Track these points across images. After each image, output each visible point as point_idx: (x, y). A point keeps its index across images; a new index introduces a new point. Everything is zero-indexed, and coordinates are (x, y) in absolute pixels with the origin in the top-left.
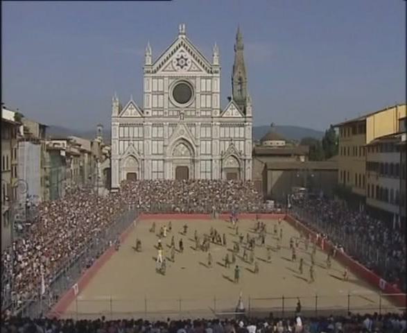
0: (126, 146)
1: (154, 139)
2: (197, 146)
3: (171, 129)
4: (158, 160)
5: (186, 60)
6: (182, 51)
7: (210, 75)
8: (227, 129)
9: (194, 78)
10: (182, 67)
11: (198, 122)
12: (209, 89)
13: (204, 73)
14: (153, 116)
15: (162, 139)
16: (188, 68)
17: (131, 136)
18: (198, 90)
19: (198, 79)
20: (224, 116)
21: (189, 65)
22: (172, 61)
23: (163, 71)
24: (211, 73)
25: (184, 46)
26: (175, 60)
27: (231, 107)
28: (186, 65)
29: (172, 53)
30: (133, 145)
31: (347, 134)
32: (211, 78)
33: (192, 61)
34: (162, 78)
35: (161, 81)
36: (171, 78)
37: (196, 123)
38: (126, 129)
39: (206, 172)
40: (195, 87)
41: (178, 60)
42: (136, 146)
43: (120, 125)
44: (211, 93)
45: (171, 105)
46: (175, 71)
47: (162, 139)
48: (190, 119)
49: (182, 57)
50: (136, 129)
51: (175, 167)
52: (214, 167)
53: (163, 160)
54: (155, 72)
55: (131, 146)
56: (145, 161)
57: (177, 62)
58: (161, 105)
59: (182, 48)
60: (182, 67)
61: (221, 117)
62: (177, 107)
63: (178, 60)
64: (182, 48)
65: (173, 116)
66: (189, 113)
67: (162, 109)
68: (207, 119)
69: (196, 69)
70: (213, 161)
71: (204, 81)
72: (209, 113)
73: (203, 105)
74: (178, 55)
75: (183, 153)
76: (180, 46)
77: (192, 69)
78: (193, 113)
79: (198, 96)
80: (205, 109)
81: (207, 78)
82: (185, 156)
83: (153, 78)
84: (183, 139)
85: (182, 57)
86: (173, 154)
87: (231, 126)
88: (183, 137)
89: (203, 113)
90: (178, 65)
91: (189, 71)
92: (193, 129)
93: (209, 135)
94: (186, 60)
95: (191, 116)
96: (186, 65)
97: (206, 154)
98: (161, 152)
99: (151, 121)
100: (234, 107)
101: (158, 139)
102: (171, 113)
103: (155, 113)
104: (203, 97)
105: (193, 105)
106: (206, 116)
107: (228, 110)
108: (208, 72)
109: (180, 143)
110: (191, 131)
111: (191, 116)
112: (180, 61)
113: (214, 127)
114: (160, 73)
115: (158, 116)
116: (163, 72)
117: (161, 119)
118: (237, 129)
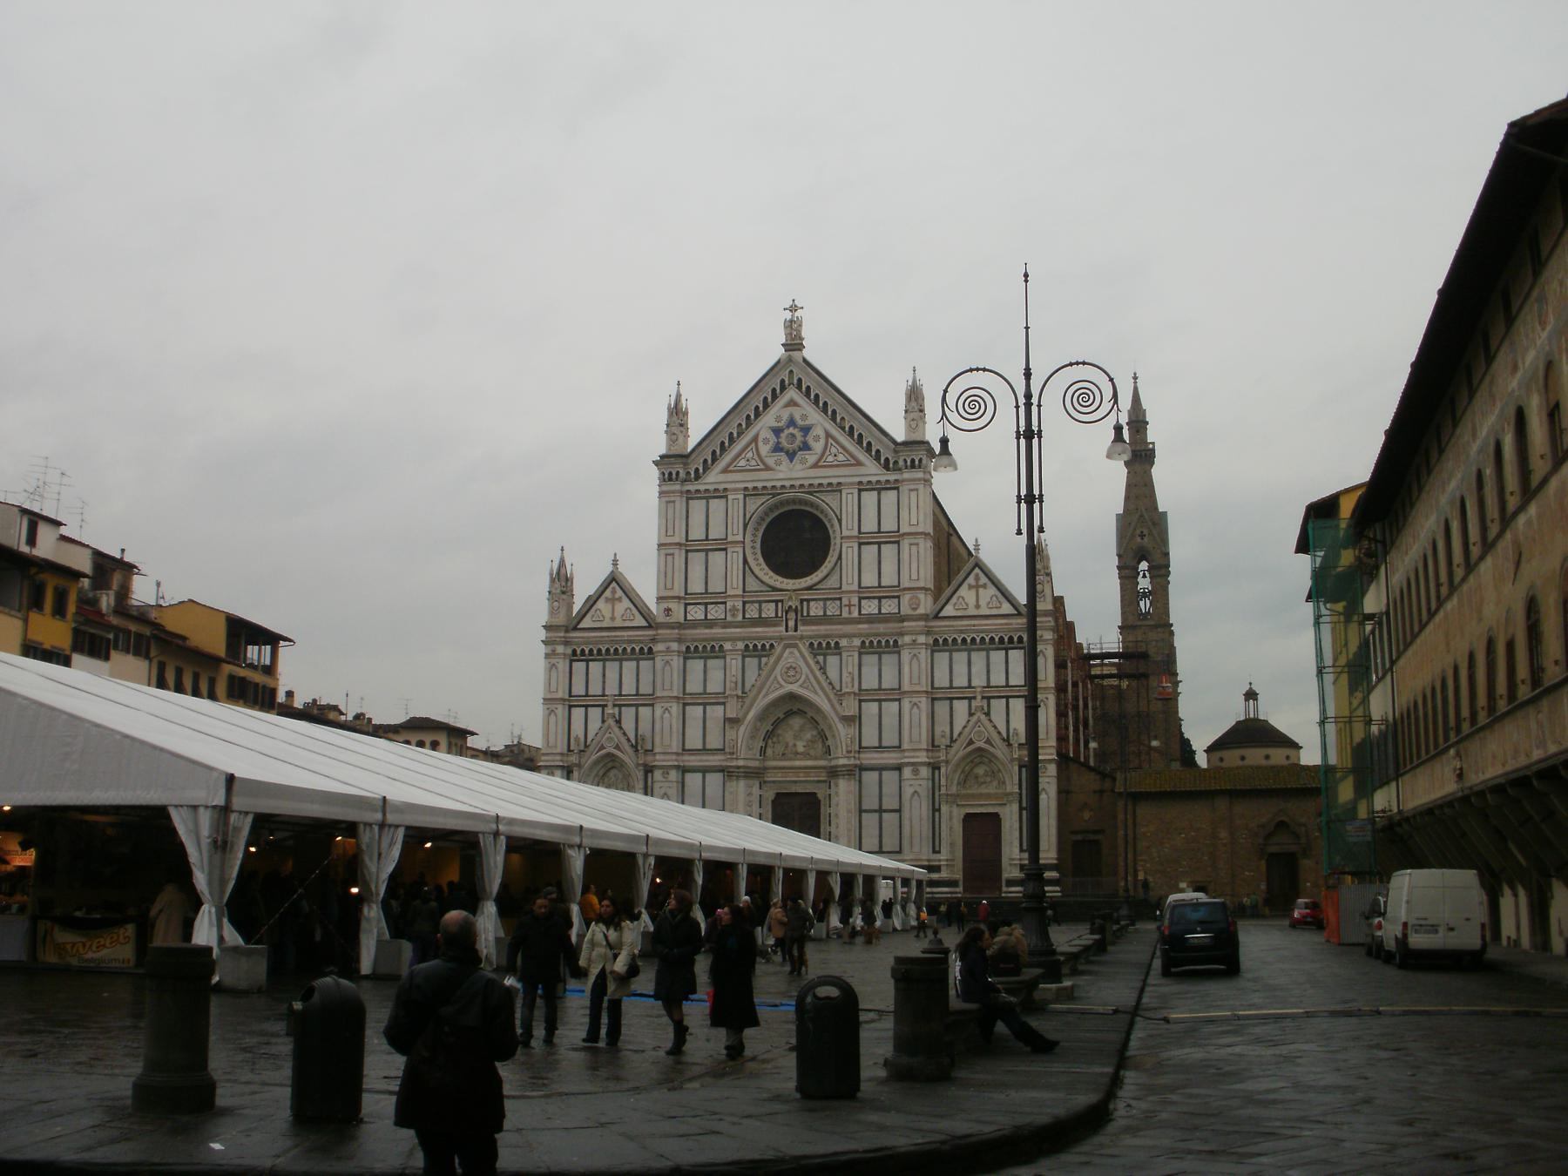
0: (595, 724)
1: (685, 701)
2: (847, 720)
3: (752, 663)
4: (705, 771)
5: (806, 430)
6: (792, 403)
7: (892, 477)
8: (960, 658)
9: (836, 489)
10: (791, 456)
11: (850, 636)
12: (889, 525)
13: (871, 470)
14: (688, 624)
15: (720, 699)
16: (812, 459)
17: (612, 690)
18: (849, 527)
19: (849, 498)
20: (949, 610)
21: (818, 447)
22: (755, 439)
23: (725, 471)
24: (897, 469)
25: (799, 386)
26: (766, 434)
27: (971, 580)
28: (806, 447)
29: (757, 414)
30: (619, 722)
31: (1450, 683)
32: (895, 487)
33: (828, 435)
34: (721, 494)
35: (716, 505)
36: (749, 493)
37: (844, 643)
38: (595, 667)
39: (880, 811)
40: (840, 521)
41: (777, 431)
42: (629, 725)
43: (574, 657)
44: (896, 538)
45: (752, 584)
46: (768, 468)
47: (720, 699)
48: (823, 629)
49: (792, 422)
50: (629, 666)
51: (770, 795)
52: (908, 791)
53: (721, 770)
54: (698, 477)
55: (611, 722)
56: (658, 774)
57: (773, 439)
58: (716, 586)
59: (792, 393)
60: (791, 456)
61: (936, 617)
62: (775, 589)
63: (777, 431)
64: (792, 393)
65: (761, 621)
66: (816, 610)
67: (721, 599)
68: (881, 627)
69: (841, 457)
70: (907, 772)
71: (870, 498)
72: (889, 607)
73: (869, 579)
74: (778, 419)
75: (801, 749)
76: (783, 388)
77: (830, 459)
78: (832, 609)
79: (850, 552)
80: (880, 593)
81: (880, 488)
82: (806, 756)
83: (690, 496)
84: (792, 697)
85: (792, 422)
86: (763, 751)
87: (969, 645)
88: (795, 688)
89: (870, 607)
90: (777, 448)
91: (815, 466)
92: (832, 661)
93: (889, 681)
94: (806, 430)
95: (825, 619)
96: (806, 447)
97: (880, 747)
98: (714, 742)
99: (679, 640)
100: (983, 580)
101: (706, 700)
102: (752, 612)
103: (697, 613)
104: (870, 552)
105: (833, 582)
106: (880, 618)
107: (963, 591)
108: (886, 466)
109: (790, 714)
110: (823, 669)
111: (825, 619)
112: (783, 435)
113: (906, 655)
114: (713, 478)
115: (708, 623)
116: (722, 477)
117: (717, 631)
118: (997, 657)
